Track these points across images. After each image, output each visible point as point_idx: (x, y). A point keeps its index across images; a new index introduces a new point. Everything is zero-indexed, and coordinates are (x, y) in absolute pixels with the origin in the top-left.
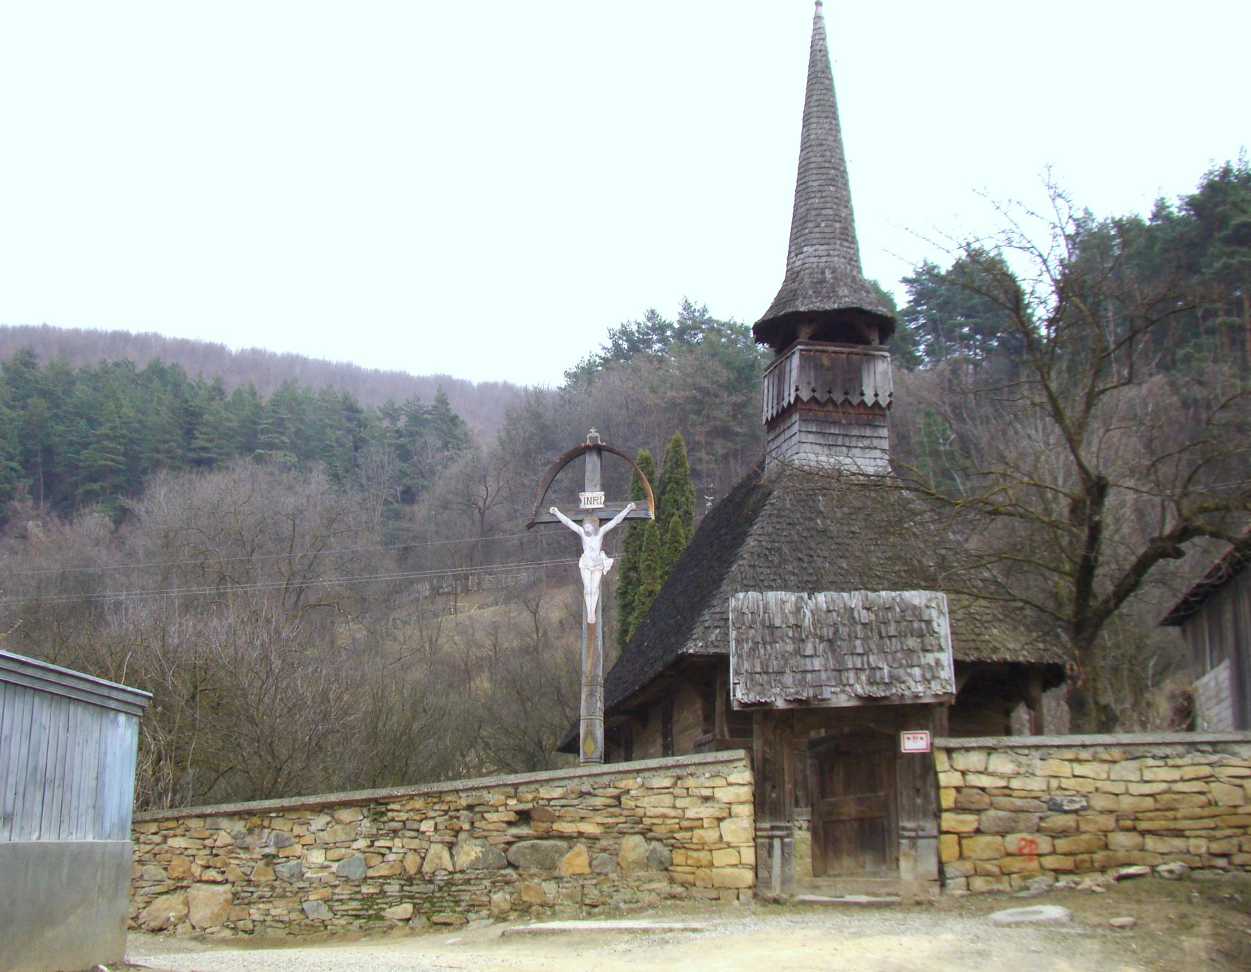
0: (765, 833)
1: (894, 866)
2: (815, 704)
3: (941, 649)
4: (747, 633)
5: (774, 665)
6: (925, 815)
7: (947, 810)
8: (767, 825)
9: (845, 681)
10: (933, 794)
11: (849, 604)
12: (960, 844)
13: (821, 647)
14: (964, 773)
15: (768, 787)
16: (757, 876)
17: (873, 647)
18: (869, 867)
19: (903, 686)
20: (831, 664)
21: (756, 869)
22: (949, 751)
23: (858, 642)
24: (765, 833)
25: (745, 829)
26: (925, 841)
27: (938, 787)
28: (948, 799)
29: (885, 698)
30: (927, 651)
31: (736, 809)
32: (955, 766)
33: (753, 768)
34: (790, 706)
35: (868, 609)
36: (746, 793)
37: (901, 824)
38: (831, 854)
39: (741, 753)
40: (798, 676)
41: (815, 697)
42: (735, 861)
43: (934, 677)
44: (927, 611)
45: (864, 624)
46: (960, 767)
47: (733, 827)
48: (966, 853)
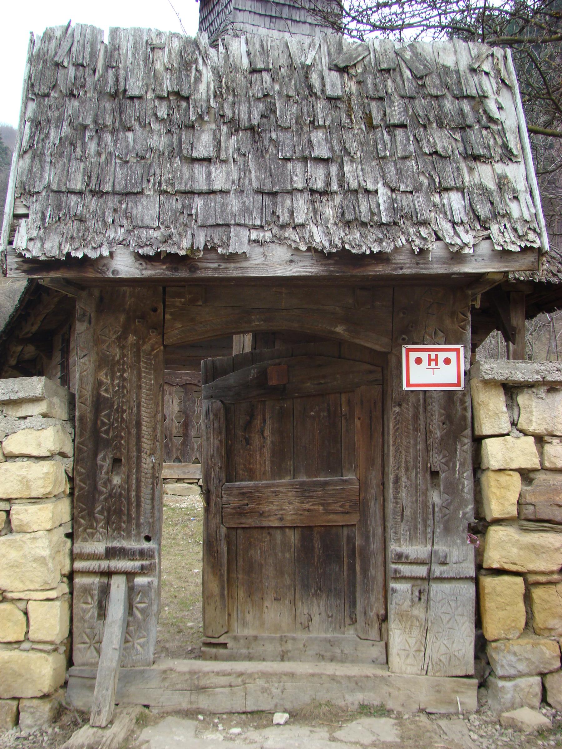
0: (92, 565)
1: (374, 633)
2: (210, 269)
3: (508, 156)
4: (61, 107)
5: (117, 177)
6: (447, 530)
7: (498, 522)
8: (99, 547)
9: (285, 218)
10: (468, 484)
11: (299, 59)
12: (528, 598)
13: (231, 145)
14: (540, 440)
15: (104, 461)
16: (70, 663)
17: (353, 146)
18: (320, 632)
19: (424, 232)
20: (255, 179)
21: (69, 650)
22: (511, 390)
23: (318, 136)
24: (92, 565)
25: (42, 560)
26: (446, 587)
27: (478, 466)
28: (502, 497)
29: (380, 257)
30: (476, 158)
31: (22, 514)
32: (523, 424)
33: (72, 419)
34: (148, 272)
35: (343, 70)
36: (47, 476)
37: (394, 547)
38: (241, 593)
39: (35, 385)
40: (173, 204)
41: (210, 249)
42: (16, 634)
43: (496, 216)
44: (473, 80)
45: (330, 99)
46: (533, 428)
47: (13, 555)
48: (540, 619)
